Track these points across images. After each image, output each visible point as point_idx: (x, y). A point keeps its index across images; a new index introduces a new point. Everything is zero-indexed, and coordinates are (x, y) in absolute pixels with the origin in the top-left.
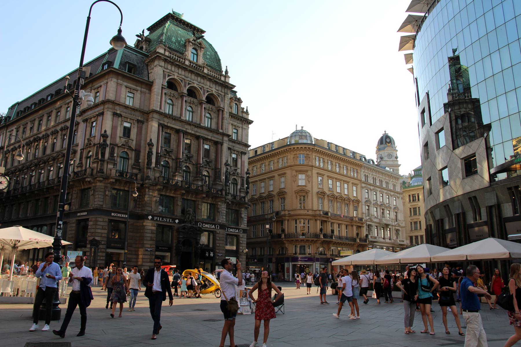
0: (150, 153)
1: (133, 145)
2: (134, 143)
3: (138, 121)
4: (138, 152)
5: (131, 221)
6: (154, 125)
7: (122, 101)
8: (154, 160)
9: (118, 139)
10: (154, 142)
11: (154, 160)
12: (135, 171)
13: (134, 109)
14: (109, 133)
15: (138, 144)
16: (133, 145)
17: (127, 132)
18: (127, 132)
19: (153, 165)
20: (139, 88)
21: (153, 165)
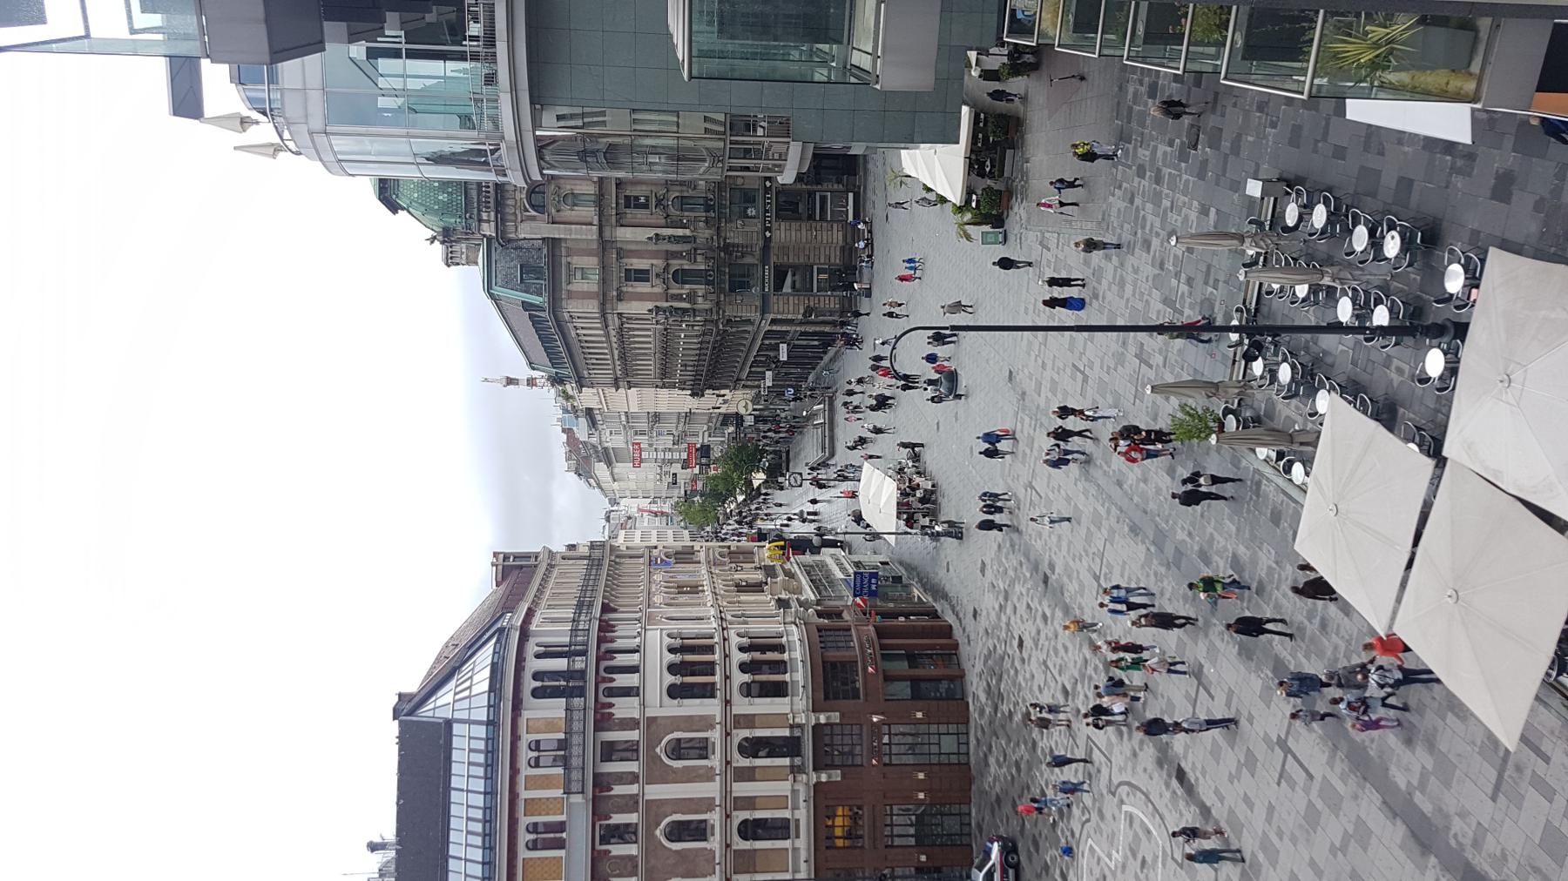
0: (670, 238)
1: (659, 263)
2: (654, 262)
3: (620, 256)
4: (670, 255)
5: (773, 259)
6: (625, 234)
7: (595, 288)
8: (680, 232)
9: (656, 290)
10: (652, 232)
11: (680, 232)
12: (699, 258)
13: (604, 267)
14: (650, 305)
15: (654, 255)
16: (659, 263)
17: (642, 276)
18: (642, 276)
19: (687, 232)
20: (564, 260)
21: (687, 232)
